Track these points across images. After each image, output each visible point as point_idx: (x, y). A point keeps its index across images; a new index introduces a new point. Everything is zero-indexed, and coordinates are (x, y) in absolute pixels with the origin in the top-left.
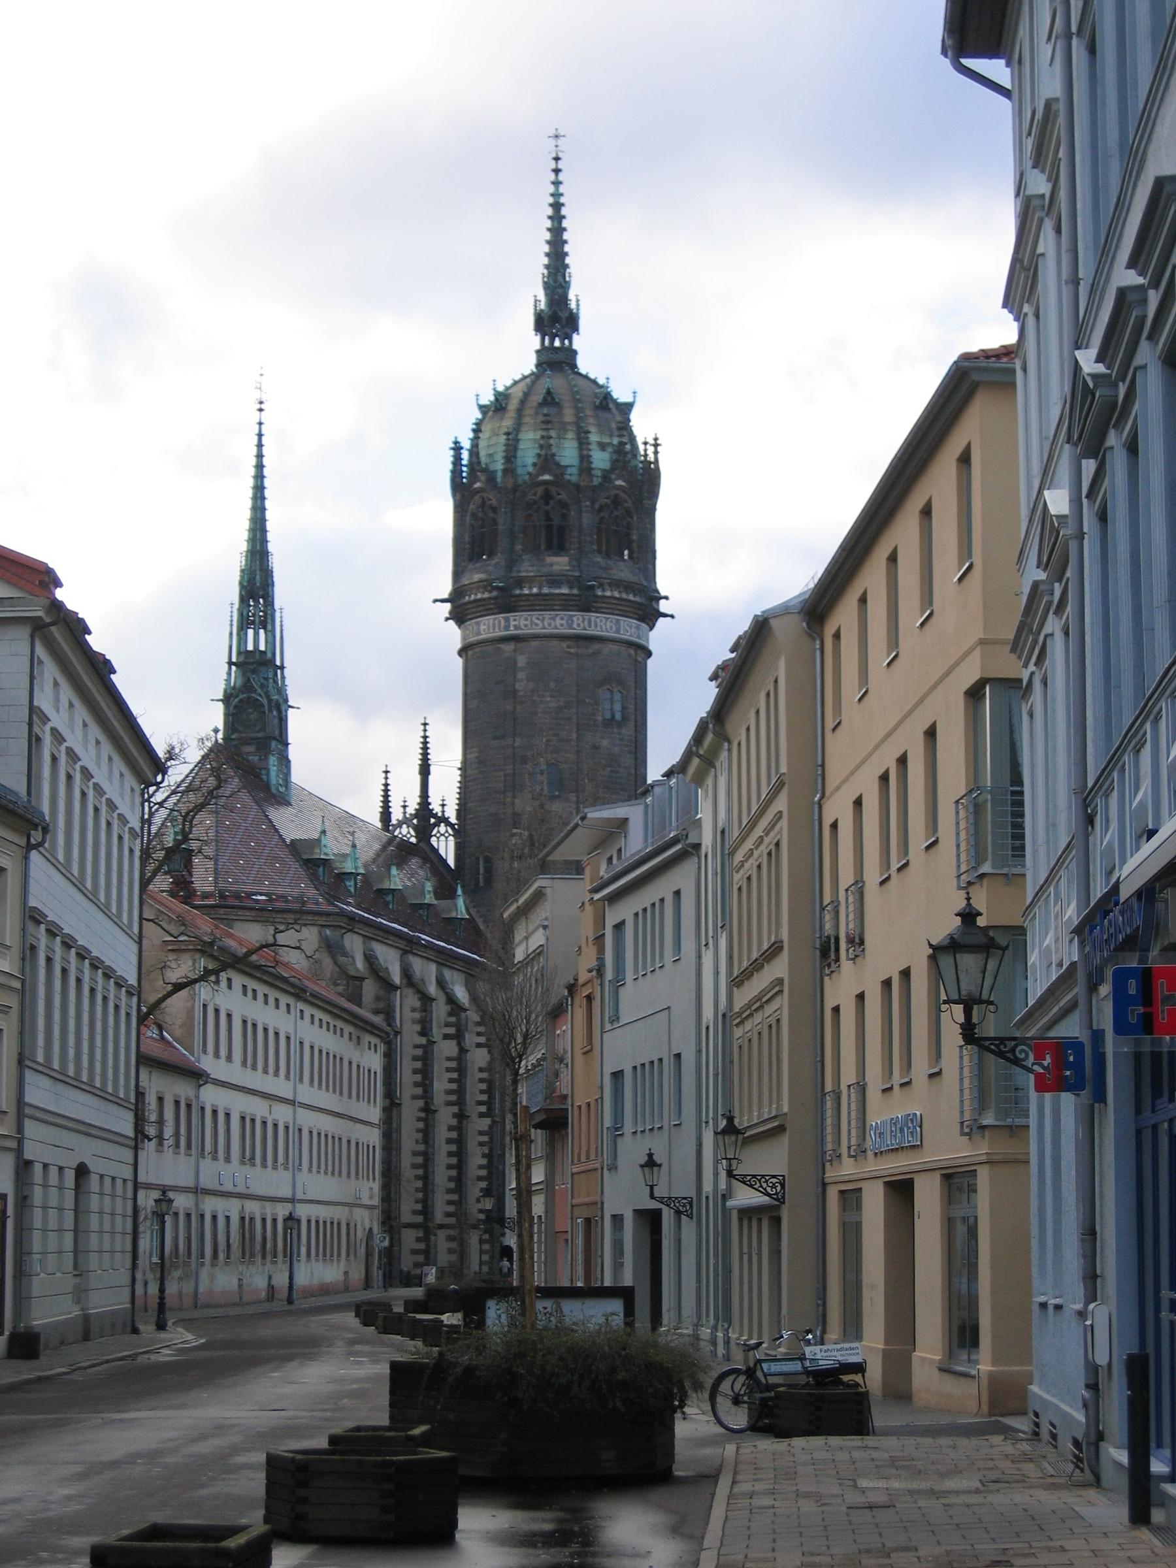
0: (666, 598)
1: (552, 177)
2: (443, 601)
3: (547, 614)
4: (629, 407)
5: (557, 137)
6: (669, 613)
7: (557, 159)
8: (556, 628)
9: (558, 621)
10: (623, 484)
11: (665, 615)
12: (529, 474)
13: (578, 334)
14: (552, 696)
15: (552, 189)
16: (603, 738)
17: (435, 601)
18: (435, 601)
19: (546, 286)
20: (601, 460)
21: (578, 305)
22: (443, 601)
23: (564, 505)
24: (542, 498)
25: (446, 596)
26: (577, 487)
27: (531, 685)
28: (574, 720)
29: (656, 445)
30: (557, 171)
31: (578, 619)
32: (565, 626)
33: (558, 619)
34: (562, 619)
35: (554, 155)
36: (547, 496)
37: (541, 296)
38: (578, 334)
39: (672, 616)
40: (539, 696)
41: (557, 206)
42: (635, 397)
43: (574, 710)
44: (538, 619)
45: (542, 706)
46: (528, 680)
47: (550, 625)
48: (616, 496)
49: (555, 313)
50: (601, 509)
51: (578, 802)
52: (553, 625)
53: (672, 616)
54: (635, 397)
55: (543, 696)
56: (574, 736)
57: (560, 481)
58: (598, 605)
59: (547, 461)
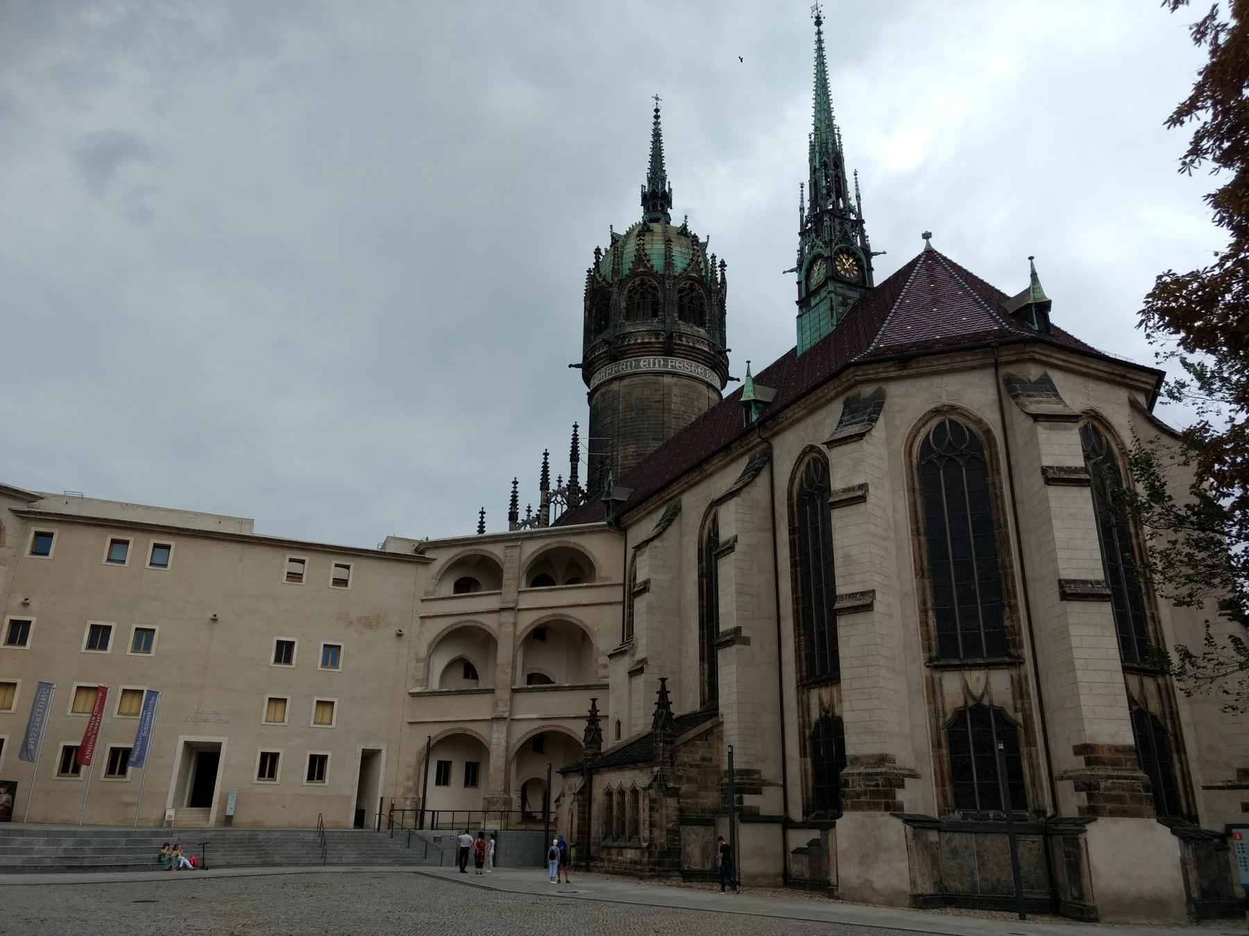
1: (654, 120)
2: (577, 366)
4: (705, 245)
5: (657, 99)
7: (657, 110)
10: (696, 276)
12: (630, 269)
13: (671, 208)
15: (653, 127)
17: (571, 366)
18: (571, 366)
19: (650, 180)
20: (680, 261)
21: (670, 190)
22: (577, 366)
23: (655, 289)
24: (639, 285)
26: (663, 276)
30: (657, 117)
35: (655, 108)
36: (642, 284)
37: (646, 184)
38: (671, 208)
41: (657, 135)
42: (708, 238)
49: (654, 190)
50: (680, 291)
54: (708, 238)
57: (650, 272)
59: (641, 258)
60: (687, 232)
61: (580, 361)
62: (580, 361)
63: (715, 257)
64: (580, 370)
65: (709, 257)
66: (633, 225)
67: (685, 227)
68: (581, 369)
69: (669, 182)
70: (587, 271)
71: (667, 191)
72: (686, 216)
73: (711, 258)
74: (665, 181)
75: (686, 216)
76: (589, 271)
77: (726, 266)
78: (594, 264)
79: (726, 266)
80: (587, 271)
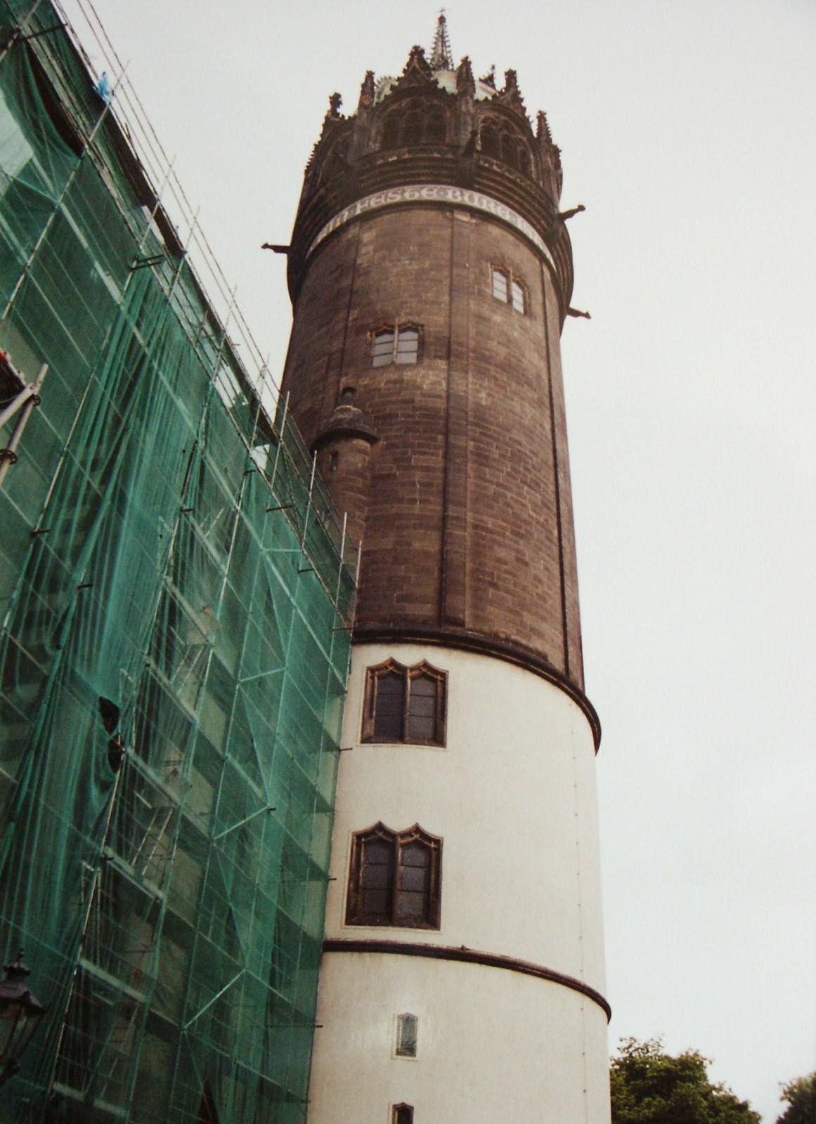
0: (581, 208)
2: (278, 249)
11: (576, 314)
14: (411, 259)
16: (493, 311)
17: (266, 246)
18: (266, 246)
22: (278, 249)
27: (379, 254)
28: (447, 282)
31: (454, 192)
36: (415, 105)
39: (587, 316)
40: (391, 261)
43: (446, 273)
44: (394, 193)
45: (395, 270)
46: (375, 251)
48: (506, 122)
51: (449, 370)
53: (587, 316)
55: (399, 260)
56: (446, 298)
58: (485, 181)
61: (287, 241)
62: (287, 241)
64: (283, 258)
72: (493, 67)
75: (493, 67)
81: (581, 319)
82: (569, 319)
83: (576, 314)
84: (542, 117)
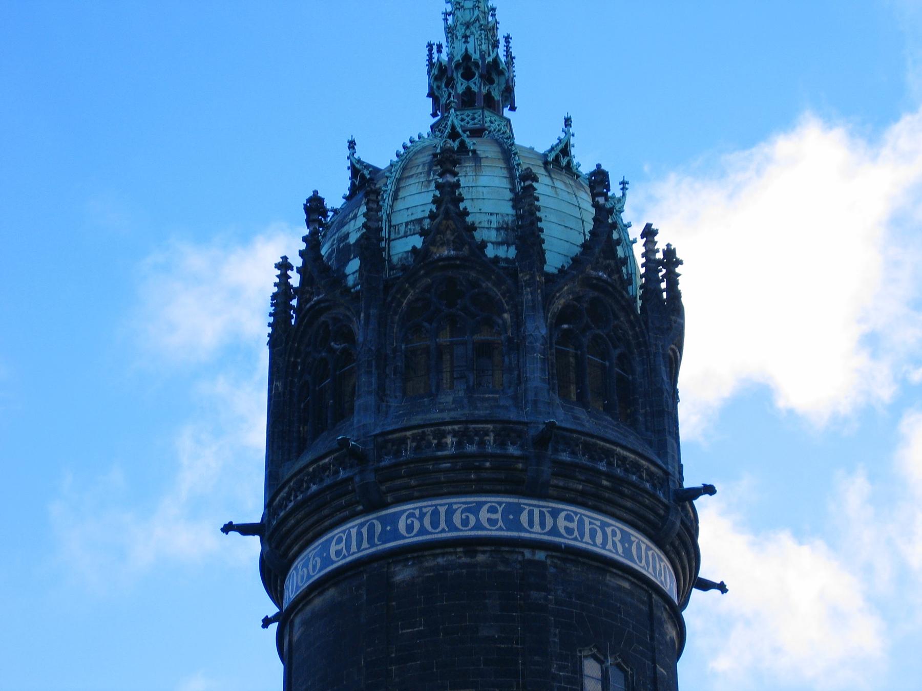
3: (459, 502)
6: (718, 582)
8: (478, 526)
9: (484, 515)
11: (705, 585)
17: (228, 528)
18: (228, 528)
22: (246, 530)
25: (256, 518)
29: (671, 259)
32: (500, 523)
33: (486, 507)
34: (493, 510)
37: (440, 37)
38: (513, 108)
39: (722, 587)
42: (624, 189)
47: (465, 522)
52: (472, 520)
53: (722, 587)
54: (624, 189)
60: (569, 163)
63: (655, 233)
64: (256, 539)
65: (635, 232)
66: (405, 147)
67: (565, 150)
68: (256, 539)
69: (507, 39)
70: (278, 266)
71: (503, 59)
72: (568, 122)
73: (642, 236)
74: (494, 35)
75: (568, 122)
76: (284, 266)
77: (679, 262)
78: (305, 239)
79: (679, 262)
80: (278, 266)
81: (715, 592)
82: (696, 594)
83: (705, 585)
84: (649, 233)
